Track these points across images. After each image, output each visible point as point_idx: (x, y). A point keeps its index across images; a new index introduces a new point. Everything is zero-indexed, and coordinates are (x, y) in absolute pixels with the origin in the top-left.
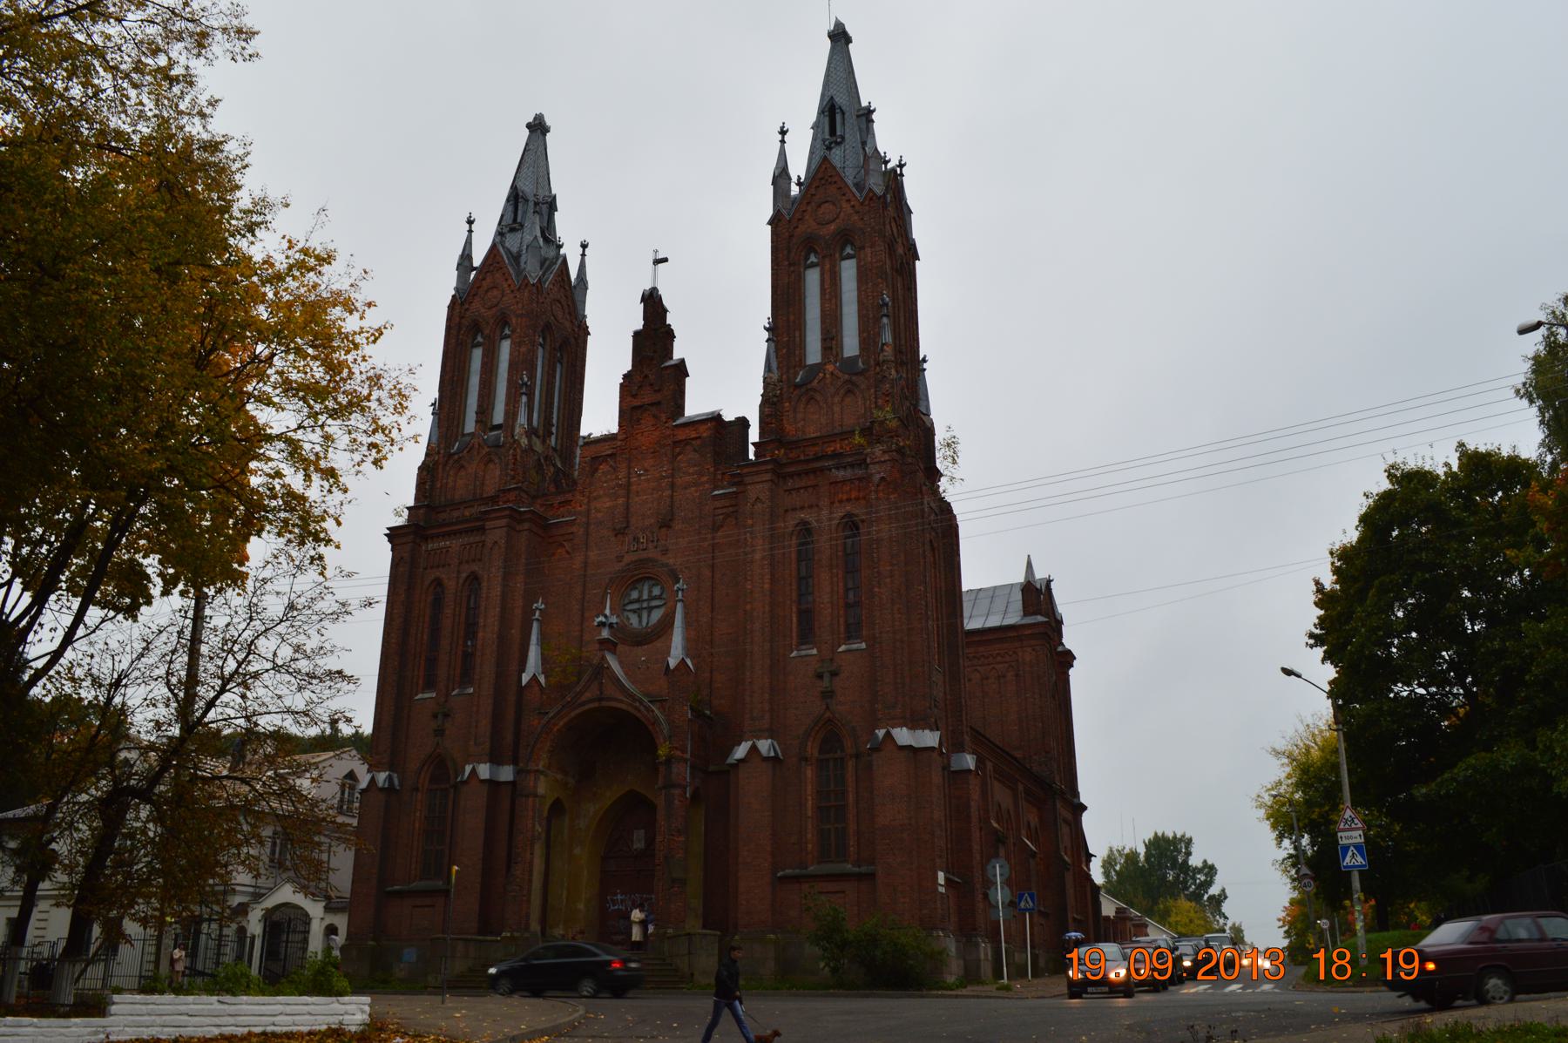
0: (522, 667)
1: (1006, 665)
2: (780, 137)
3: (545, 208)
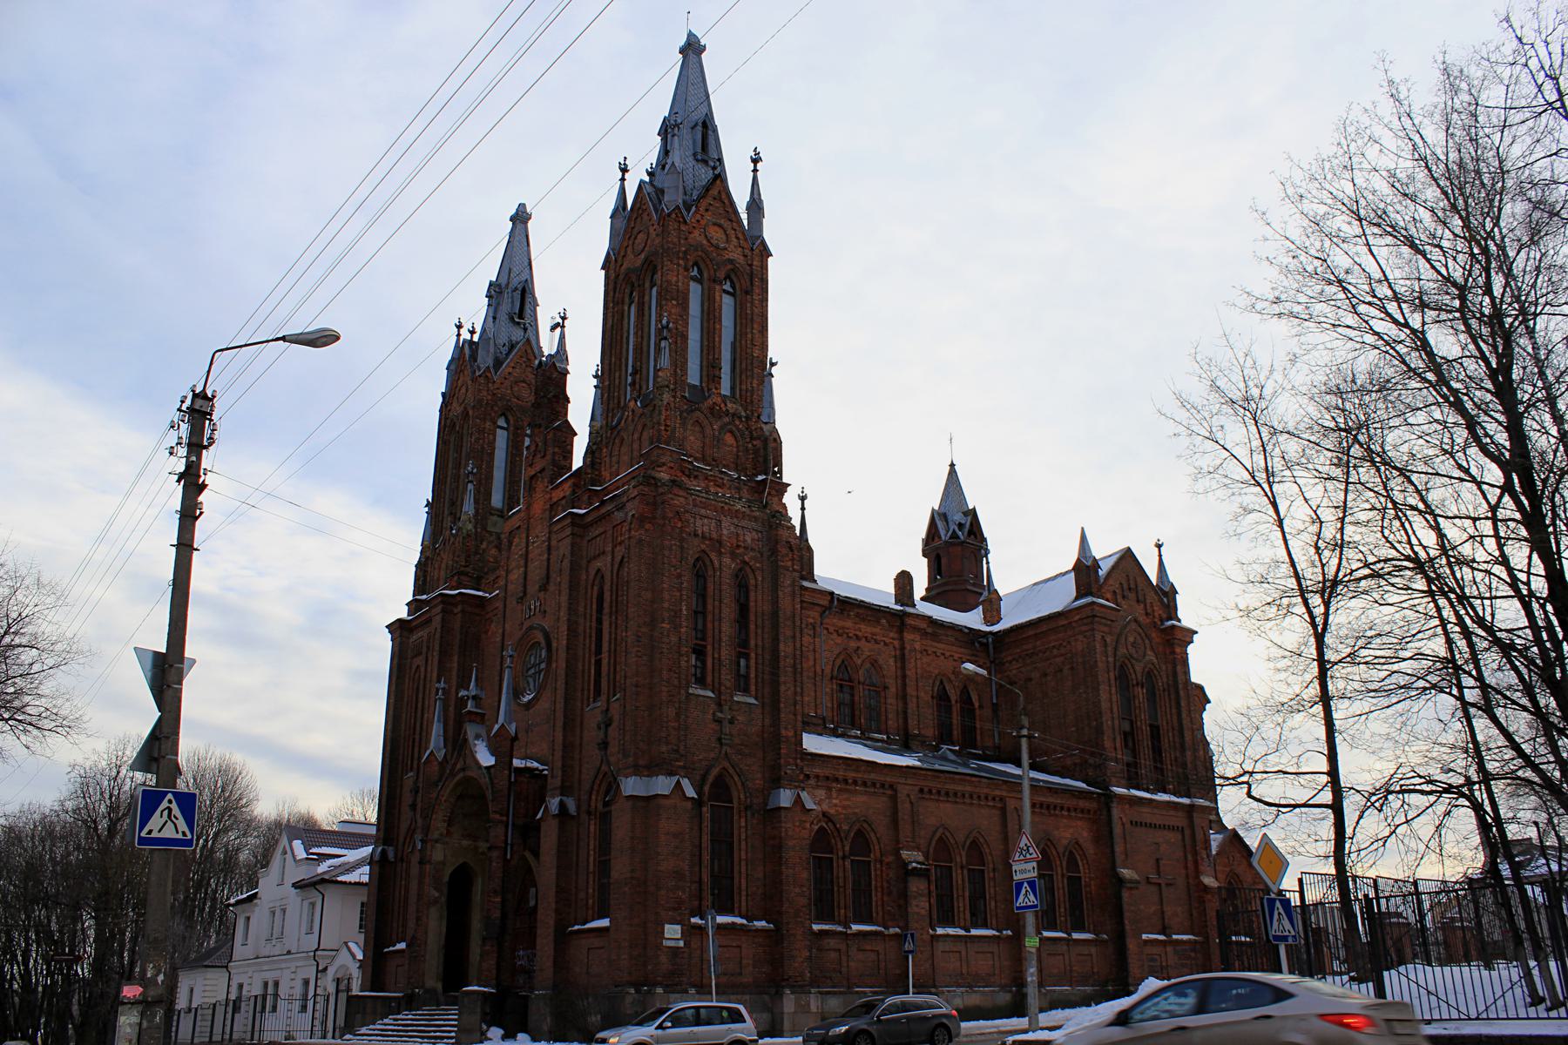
0: (423, 742)
1: (1062, 658)
2: (620, 175)
3: (517, 295)
